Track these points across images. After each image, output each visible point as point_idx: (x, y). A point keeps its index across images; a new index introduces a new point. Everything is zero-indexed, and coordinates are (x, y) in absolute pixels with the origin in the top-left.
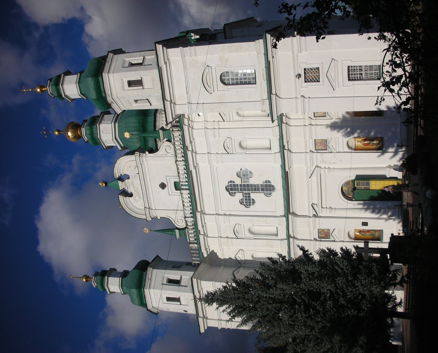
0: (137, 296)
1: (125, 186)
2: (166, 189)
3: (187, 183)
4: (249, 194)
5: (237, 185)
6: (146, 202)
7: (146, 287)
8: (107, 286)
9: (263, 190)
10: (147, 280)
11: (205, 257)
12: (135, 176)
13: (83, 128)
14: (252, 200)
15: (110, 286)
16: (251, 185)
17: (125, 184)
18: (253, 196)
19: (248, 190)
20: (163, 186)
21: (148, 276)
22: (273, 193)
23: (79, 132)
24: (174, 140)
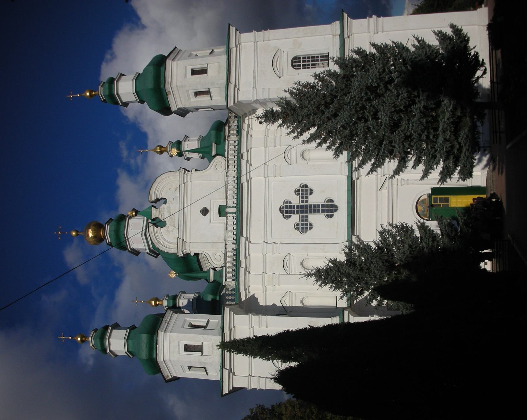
0: (146, 347)
1: (159, 214)
2: (208, 215)
3: (234, 210)
4: (307, 217)
5: (294, 206)
6: (181, 231)
7: (161, 329)
8: (109, 339)
9: (323, 211)
10: (164, 322)
11: (242, 300)
12: (173, 199)
13: (108, 225)
14: (310, 225)
15: (112, 340)
16: (311, 206)
17: (159, 212)
19: (306, 212)
21: (166, 318)
22: (335, 214)
23: (101, 233)
24: (228, 148)
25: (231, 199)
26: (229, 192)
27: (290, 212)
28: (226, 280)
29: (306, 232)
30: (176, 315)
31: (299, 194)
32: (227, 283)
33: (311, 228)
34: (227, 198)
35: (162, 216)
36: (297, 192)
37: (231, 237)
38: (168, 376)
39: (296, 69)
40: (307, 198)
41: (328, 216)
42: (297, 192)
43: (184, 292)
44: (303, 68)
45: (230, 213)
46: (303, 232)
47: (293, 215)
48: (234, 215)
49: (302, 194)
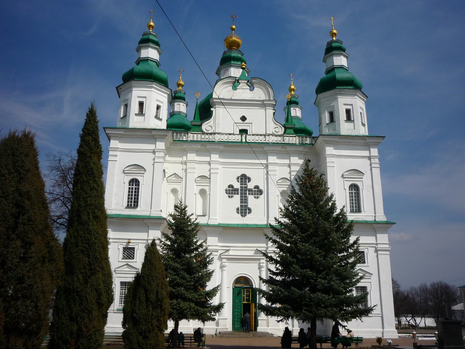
1: (243, 85)
2: (241, 121)
4: (238, 194)
9: (241, 206)
16: (246, 197)
18: (237, 198)
19: (241, 194)
22: (240, 215)
24: (290, 136)
25: (252, 138)
26: (257, 137)
27: (241, 182)
29: (227, 193)
30: (166, 96)
31: (255, 188)
32: (189, 134)
33: (229, 197)
34: (253, 135)
37: (224, 138)
38: (121, 89)
39: (349, 187)
40: (252, 194)
41: (238, 209)
42: (257, 187)
43: (187, 106)
44: (350, 192)
45: (241, 137)
46: (226, 190)
47: (239, 183)
48: (240, 140)
49: (255, 191)
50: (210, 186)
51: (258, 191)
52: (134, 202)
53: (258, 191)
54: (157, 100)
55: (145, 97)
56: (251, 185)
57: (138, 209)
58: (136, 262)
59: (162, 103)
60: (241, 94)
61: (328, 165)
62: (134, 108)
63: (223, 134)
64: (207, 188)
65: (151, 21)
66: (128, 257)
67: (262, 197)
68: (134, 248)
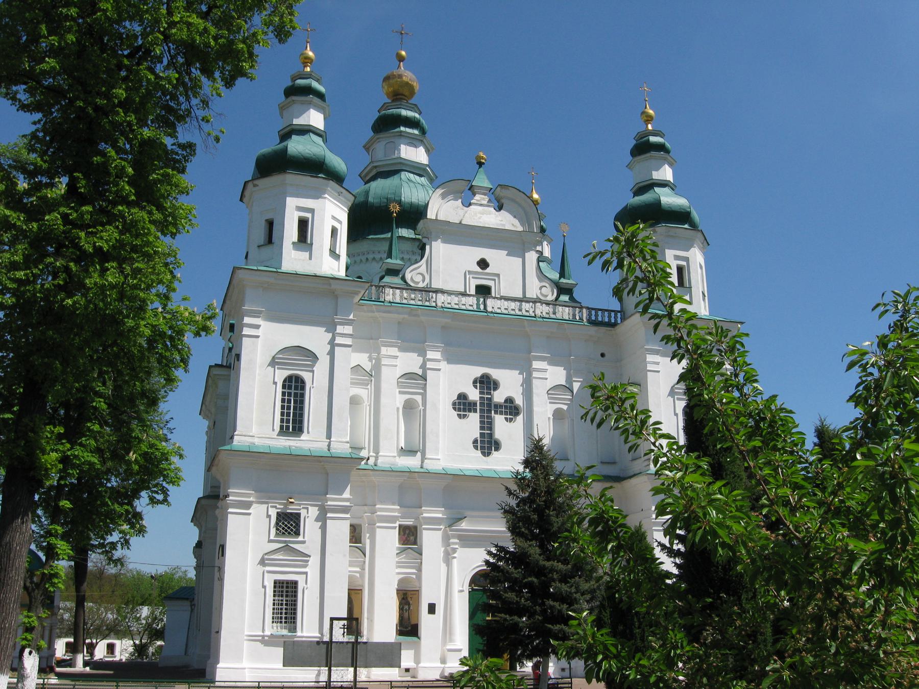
2: (478, 269)
4: (475, 411)
5: (490, 394)
9: (482, 435)
16: (490, 417)
18: (474, 419)
20: (483, 264)
22: (479, 453)
28: (392, 288)
29: (455, 409)
31: (506, 401)
33: (459, 416)
34: (502, 298)
35: (477, 200)
36: (509, 400)
40: (501, 413)
41: (475, 441)
42: (509, 400)
46: (454, 404)
47: (478, 391)
50: (424, 396)
51: (510, 409)
52: (294, 421)
53: (510, 409)
54: (334, 218)
55: (312, 211)
56: (499, 397)
57: (304, 437)
58: (304, 542)
59: (340, 222)
60: (479, 215)
61: (649, 367)
62: (291, 232)
63: (449, 293)
64: (419, 398)
65: (308, 48)
66: (286, 531)
67: (520, 418)
68: (299, 515)
